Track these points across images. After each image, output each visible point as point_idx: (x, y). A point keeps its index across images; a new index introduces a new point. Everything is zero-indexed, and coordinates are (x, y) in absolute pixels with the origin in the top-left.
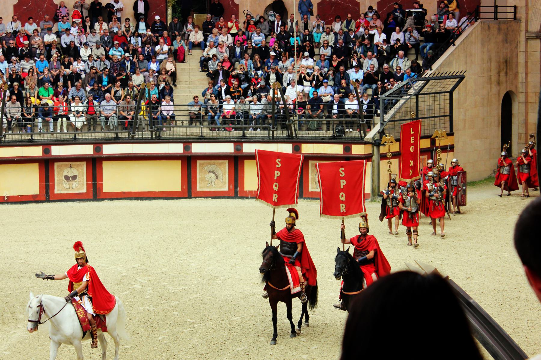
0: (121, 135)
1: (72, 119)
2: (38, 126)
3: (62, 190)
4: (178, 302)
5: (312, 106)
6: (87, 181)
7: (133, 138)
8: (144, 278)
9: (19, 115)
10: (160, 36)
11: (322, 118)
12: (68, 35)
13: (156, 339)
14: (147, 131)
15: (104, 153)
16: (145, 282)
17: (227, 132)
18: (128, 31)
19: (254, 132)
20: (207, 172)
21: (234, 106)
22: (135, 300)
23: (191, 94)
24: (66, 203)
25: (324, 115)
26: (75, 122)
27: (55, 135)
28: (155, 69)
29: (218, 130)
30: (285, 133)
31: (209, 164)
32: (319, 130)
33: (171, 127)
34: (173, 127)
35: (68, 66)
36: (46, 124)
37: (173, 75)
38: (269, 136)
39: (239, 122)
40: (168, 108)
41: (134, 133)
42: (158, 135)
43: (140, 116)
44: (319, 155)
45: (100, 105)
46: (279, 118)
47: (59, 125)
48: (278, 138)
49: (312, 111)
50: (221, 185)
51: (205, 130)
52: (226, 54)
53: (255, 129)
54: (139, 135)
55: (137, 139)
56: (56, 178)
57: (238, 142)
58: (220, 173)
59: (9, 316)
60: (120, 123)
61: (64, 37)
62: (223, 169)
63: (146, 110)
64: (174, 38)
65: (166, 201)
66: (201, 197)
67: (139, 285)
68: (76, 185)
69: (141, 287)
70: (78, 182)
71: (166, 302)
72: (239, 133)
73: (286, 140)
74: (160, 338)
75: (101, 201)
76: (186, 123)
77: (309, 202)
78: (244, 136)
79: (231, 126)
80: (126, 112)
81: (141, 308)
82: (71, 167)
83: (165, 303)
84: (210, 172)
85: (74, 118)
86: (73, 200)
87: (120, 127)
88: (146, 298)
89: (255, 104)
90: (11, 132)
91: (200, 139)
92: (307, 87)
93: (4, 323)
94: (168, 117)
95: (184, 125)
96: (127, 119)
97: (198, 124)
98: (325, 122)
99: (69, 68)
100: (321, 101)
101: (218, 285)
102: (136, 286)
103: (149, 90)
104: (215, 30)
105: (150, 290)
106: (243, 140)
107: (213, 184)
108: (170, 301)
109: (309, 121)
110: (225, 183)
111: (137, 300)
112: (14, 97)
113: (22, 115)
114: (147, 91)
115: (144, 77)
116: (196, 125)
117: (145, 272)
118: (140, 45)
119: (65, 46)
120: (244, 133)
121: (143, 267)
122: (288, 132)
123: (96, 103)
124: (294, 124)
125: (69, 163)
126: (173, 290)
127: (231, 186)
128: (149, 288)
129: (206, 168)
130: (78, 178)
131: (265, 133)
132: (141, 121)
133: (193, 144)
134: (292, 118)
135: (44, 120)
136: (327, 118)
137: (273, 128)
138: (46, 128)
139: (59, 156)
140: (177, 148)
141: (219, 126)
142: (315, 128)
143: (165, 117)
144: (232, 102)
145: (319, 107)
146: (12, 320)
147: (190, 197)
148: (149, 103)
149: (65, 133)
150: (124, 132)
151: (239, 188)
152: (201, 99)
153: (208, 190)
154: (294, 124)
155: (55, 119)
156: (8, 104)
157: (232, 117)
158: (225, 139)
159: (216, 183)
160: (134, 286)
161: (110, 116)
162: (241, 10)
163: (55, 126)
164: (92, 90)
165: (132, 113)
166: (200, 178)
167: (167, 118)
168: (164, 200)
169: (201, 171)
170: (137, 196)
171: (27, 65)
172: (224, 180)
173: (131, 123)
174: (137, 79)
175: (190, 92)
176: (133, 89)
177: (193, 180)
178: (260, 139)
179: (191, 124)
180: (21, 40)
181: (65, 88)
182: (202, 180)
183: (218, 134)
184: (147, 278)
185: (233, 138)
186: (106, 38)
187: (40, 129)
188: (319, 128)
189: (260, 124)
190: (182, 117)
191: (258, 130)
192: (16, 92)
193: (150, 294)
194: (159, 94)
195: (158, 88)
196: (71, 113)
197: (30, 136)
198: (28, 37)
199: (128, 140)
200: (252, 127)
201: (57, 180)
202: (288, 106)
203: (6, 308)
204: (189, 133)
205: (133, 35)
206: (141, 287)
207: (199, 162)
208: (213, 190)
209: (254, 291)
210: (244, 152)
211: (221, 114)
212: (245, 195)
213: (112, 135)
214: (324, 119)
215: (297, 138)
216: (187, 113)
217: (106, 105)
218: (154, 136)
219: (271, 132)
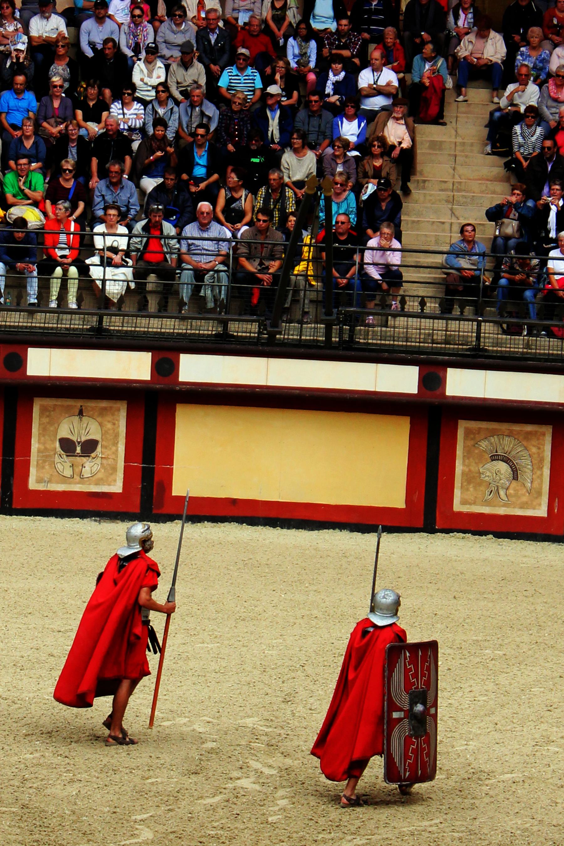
1: (96, 273)
3: (50, 481)
4: (364, 841)
6: (126, 460)
8: (270, 761)
10: (373, 40)
12: (100, 20)
14: (316, 322)
15: (182, 378)
16: (274, 772)
18: (279, 18)
20: (487, 456)
22: (237, 825)
23: (454, 220)
24: (59, 519)
26: (104, 281)
27: (39, 316)
28: (353, 139)
29: (529, 334)
31: (493, 433)
33: (387, 315)
34: (395, 316)
41: (275, 325)
42: (346, 337)
43: (297, 275)
45: (179, 234)
50: (525, 499)
55: (283, 343)
56: (35, 445)
58: (525, 463)
61: (88, 25)
62: (534, 450)
65: (357, 536)
66: (464, 532)
67: (252, 779)
68: (95, 469)
70: (98, 461)
75: (164, 522)
76: (432, 306)
80: (258, 261)
82: (81, 413)
84: (494, 458)
85: (101, 268)
86: (82, 514)
88: (270, 819)
95: (427, 310)
96: (260, 281)
97: (468, 310)
99: (98, 120)
102: (245, 783)
105: (283, 798)
107: (502, 493)
108: (340, 835)
110: (539, 494)
111: (242, 827)
114: (322, 203)
115: (320, 160)
116: (462, 312)
117: (273, 742)
118: (312, 65)
119: (89, 53)
123: (169, 228)
125: (78, 403)
128: (281, 792)
129: (484, 444)
130: (99, 448)
133: (451, 372)
138: (15, 292)
139: (49, 378)
149: (72, 312)
150: (247, 321)
153: (486, 510)
158: (546, 360)
159: (511, 491)
160: (239, 783)
161: (208, 271)
163: (44, 288)
165: (274, 266)
166: (463, 473)
168: (352, 531)
169: (468, 454)
170: (273, 514)
172: (536, 484)
175: (453, 213)
177: (442, 478)
181: (81, 180)
183: (528, 346)
184: (278, 760)
186: (213, 38)
193: (284, 809)
196: (93, 255)
199: (256, 344)
201: (39, 451)
204: (439, 336)
206: (257, 787)
207: (463, 426)
208: (502, 511)
211: (541, 286)
217: (196, 234)
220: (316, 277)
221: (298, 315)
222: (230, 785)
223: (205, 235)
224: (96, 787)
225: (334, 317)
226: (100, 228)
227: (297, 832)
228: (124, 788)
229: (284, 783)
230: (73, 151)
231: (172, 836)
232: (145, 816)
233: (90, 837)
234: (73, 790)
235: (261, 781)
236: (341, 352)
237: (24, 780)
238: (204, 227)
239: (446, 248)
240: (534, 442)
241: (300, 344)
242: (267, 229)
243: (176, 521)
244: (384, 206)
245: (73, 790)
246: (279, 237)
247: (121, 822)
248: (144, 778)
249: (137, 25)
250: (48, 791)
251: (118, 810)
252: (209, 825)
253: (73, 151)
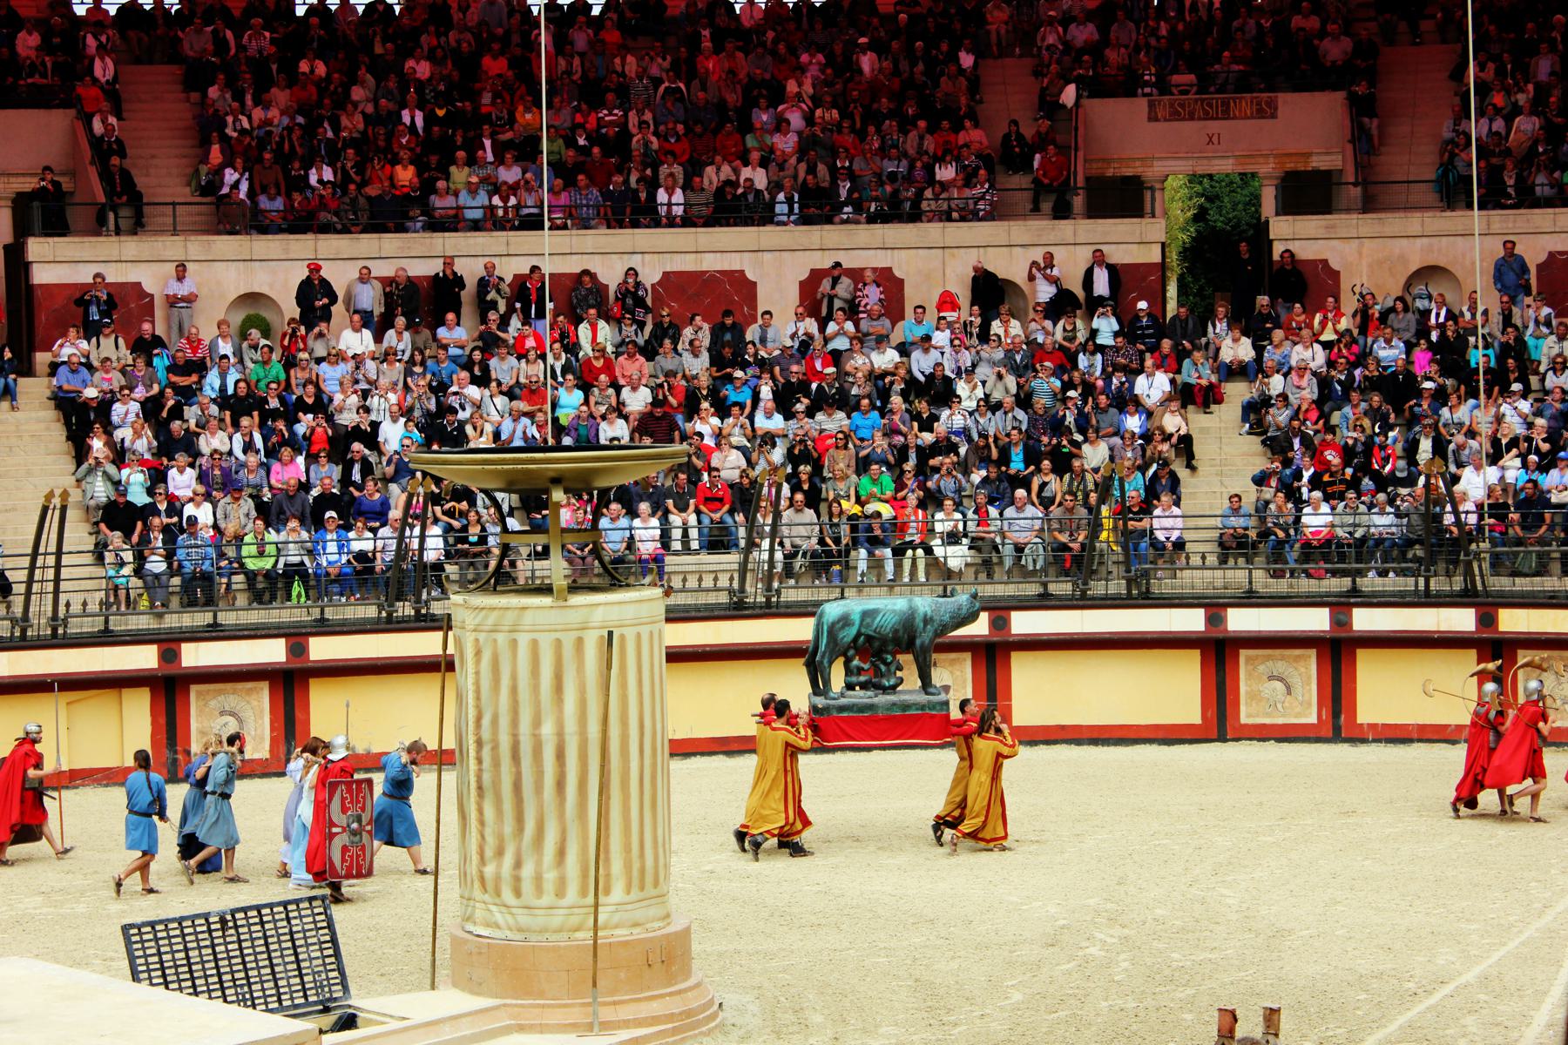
0: (1053, 588)
1: (939, 551)
2: (856, 568)
5: (1524, 517)
7: (1084, 596)
8: (1111, 932)
9: (814, 540)
10: (1148, 350)
11: (1550, 545)
12: (926, 351)
15: (1014, 631)
16: (1114, 940)
17: (1312, 581)
19: (1379, 580)
20: (1265, 678)
21: (1330, 518)
23: (1224, 490)
25: (1557, 539)
26: (945, 558)
28: (1137, 430)
29: (1292, 576)
30: (1458, 583)
31: (1269, 658)
32: (1542, 576)
33: (1175, 570)
34: (1181, 569)
35: (927, 426)
36: (876, 565)
37: (1185, 445)
38: (1416, 589)
39: (1342, 558)
40: (1168, 523)
41: (1085, 583)
42: (1144, 589)
44: (1543, 637)
45: (1001, 514)
46: (1441, 546)
47: (907, 564)
48: (1439, 594)
49: (1523, 528)
50: (1298, 709)
51: (1259, 575)
52: (1310, 392)
53: (1383, 573)
54: (1097, 588)
55: (1093, 598)
57: (1340, 606)
58: (1295, 681)
59: (790, 1017)
60: (1051, 559)
61: (916, 355)
62: (1303, 670)
63: (1115, 528)
64: (1181, 355)
65: (1165, 748)
66: (1250, 739)
67: (1098, 947)
69: (1103, 953)
72: (1342, 584)
73: (1459, 600)
76: (1212, 560)
78: (1354, 591)
79: (1322, 565)
81: (1104, 1004)
84: (1271, 678)
87: (1052, 571)
89: (1382, 513)
90: (792, 582)
91: (1248, 598)
92: (1513, 470)
93: (778, 1034)
94: (1169, 545)
95: (1208, 563)
96: (1071, 549)
97: (1241, 561)
98: (1557, 555)
99: (931, 431)
100: (1547, 504)
101: (1290, 952)
102: (1092, 950)
103: (1121, 480)
104: (1278, 334)
105: (1125, 960)
106: (1352, 600)
107: (1279, 706)
109: (1519, 552)
110: (1310, 704)
111: (1093, 985)
112: (799, 497)
113: (822, 542)
114: (1116, 483)
115: (1111, 449)
118: (1098, 373)
119: (922, 379)
120: (1354, 582)
121: (1109, 906)
122: (1465, 580)
123: (993, 512)
124: (1479, 560)
127: (1324, 712)
128: (1123, 956)
129: (1261, 668)
131: (1408, 583)
132: (1102, 555)
133: (1230, 610)
134: (1473, 546)
135: (871, 554)
136: (1562, 545)
137: (1428, 570)
138: (875, 572)
140: (1192, 621)
141: (1292, 565)
142: (1533, 571)
143: (1160, 546)
144: (1325, 508)
145: (1540, 519)
146: (795, 1028)
147: (1222, 738)
148: (1122, 512)
149: (922, 585)
151: (1343, 717)
152: (1249, 503)
153: (1267, 721)
154: (1479, 560)
155: (899, 552)
156: (787, 515)
157: (1328, 542)
159: (1286, 704)
161: (1026, 544)
162: (1345, 286)
163: (898, 567)
164: (985, 481)
166: (1247, 692)
167: (1164, 548)
169: (1249, 676)
170: (1095, 735)
171: (833, 422)
173: (1078, 560)
174: (1095, 455)
176: (1083, 478)
177: (1229, 697)
178: (1394, 596)
179: (1223, 560)
180: (818, 365)
182: (1254, 696)
183: (1291, 586)
184: (1117, 931)
185: (1328, 595)
186: (1018, 358)
187: (863, 575)
188: (1542, 571)
189: (1393, 561)
190: (1202, 545)
191: (1391, 574)
192: (806, 487)
194: (1147, 489)
195: (1144, 475)
197: (838, 590)
198: (836, 357)
200: (1376, 569)
202: (1463, 516)
203: (783, 999)
204: (1219, 583)
205: (1083, 348)
206: (1103, 953)
207: (1244, 654)
208: (1280, 721)
209: (1381, 967)
210: (1355, 627)
212: (1356, 734)
213: (1032, 589)
214: (1554, 547)
215: (1487, 594)
216: (1216, 534)
218: (1135, 592)
219: (1421, 581)
220: (1116, 542)
221: (1104, 574)
222: (1080, 953)
223: (1022, 515)
225: (1133, 573)
226: (939, 516)
230: (913, 455)
234: (954, 965)
236: (1141, 602)
237: (915, 959)
238: (1020, 509)
239: (1219, 512)
240: (1302, 663)
241: (1106, 597)
242: (1073, 508)
244: (1164, 481)
245: (954, 965)
246: (1083, 512)
248: (1011, 952)
249: (957, 353)
250: (935, 967)
253: (913, 455)
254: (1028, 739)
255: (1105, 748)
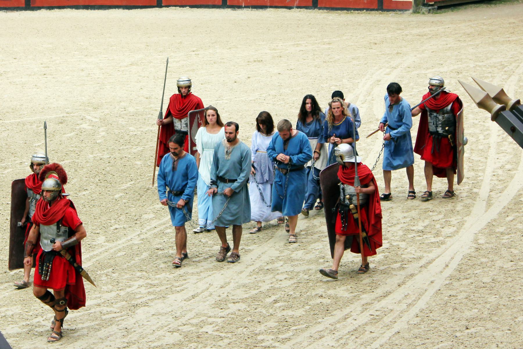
13: (112, 197)
16: (97, 120)
65: (126, 11)
67: (88, 124)
71: (125, 147)
74: (117, 196)
75: (37, 10)
77: (326, 14)
81: (92, 156)
83: (123, 149)
105: (103, 131)
111: (85, 145)
126: (135, 131)
128: (102, 129)
206: (91, 127)
222: (78, 127)
224: (16, 132)
227: (111, 147)
228: (29, 132)
229: (103, 125)
231: (53, 152)
232: (40, 144)
233: (15, 155)
235: (92, 124)
243: (42, 10)
247: (29, 147)
251: (27, 142)
252: (70, 146)
254: (48, 5)
255: (93, 11)
